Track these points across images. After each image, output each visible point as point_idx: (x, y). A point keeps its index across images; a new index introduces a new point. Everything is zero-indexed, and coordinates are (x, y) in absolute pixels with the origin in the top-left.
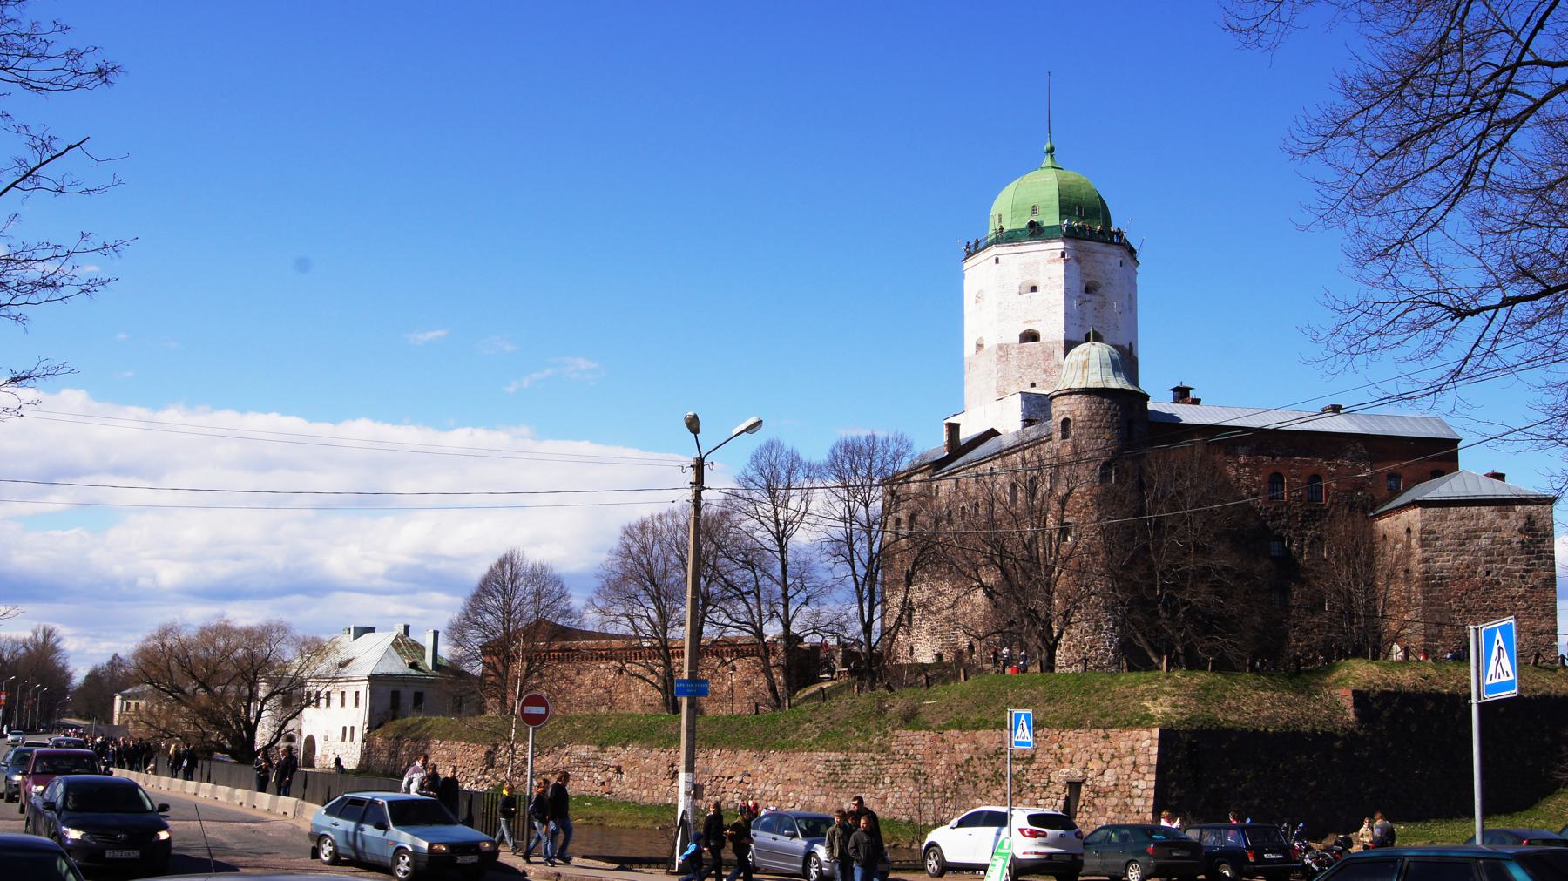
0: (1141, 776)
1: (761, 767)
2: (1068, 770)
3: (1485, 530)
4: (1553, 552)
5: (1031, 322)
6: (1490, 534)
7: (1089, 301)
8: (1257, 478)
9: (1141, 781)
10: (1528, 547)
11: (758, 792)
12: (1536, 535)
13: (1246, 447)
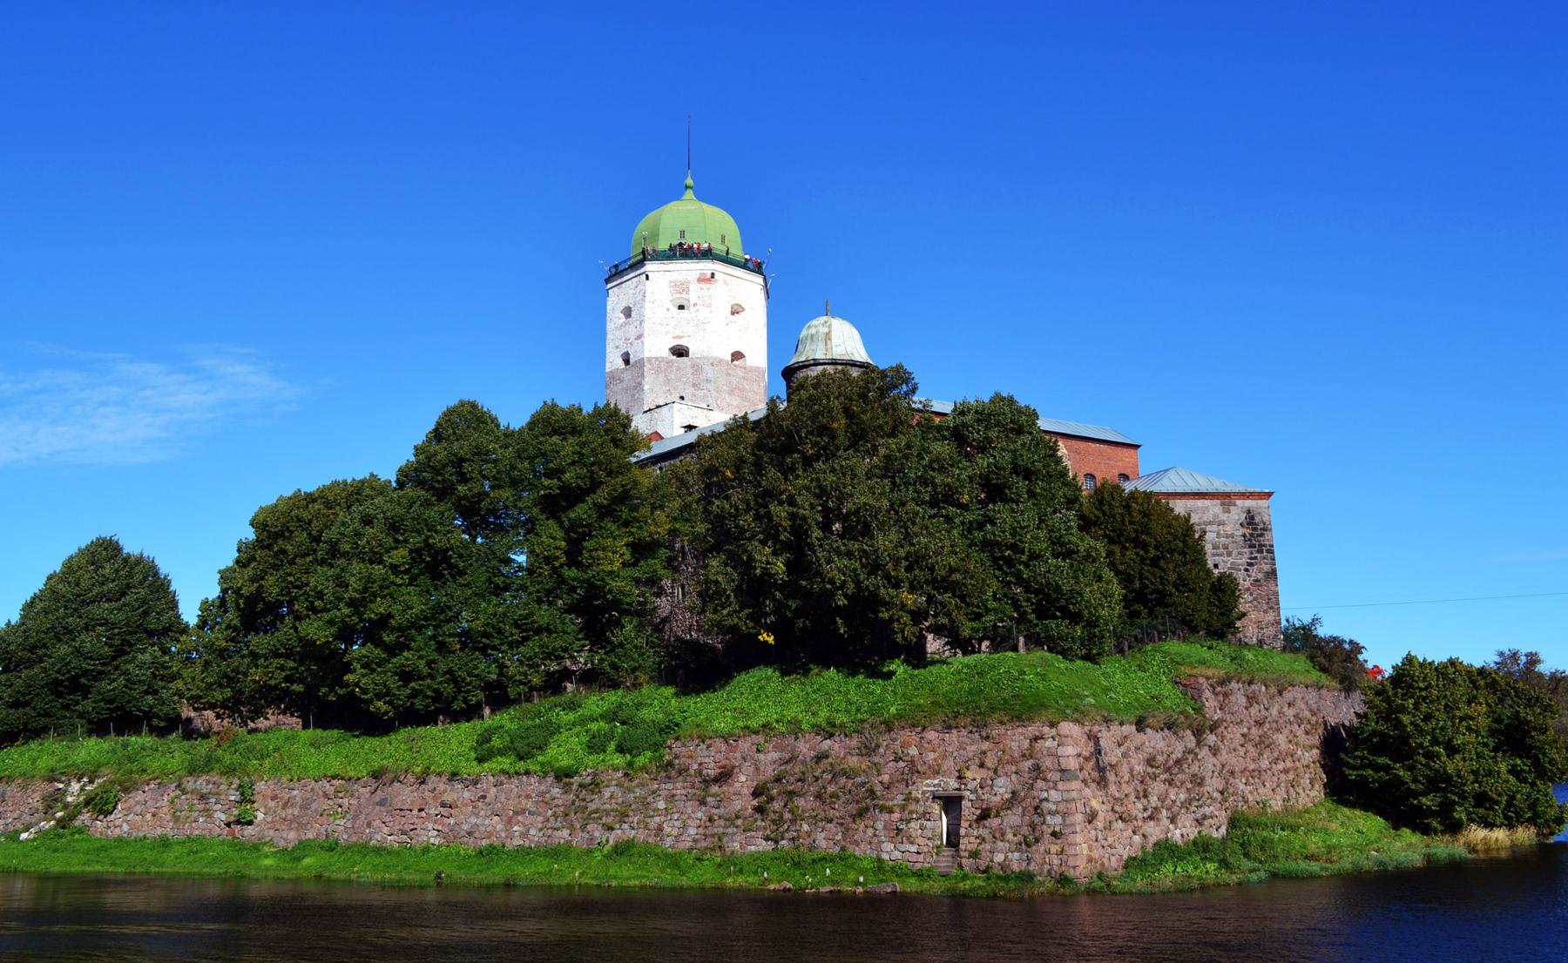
0: (1051, 784)
1: (467, 794)
2: (936, 782)
3: (1210, 523)
4: (1272, 546)
5: (680, 337)
6: (1214, 528)
9: (1052, 792)
10: (1250, 540)
11: (465, 827)
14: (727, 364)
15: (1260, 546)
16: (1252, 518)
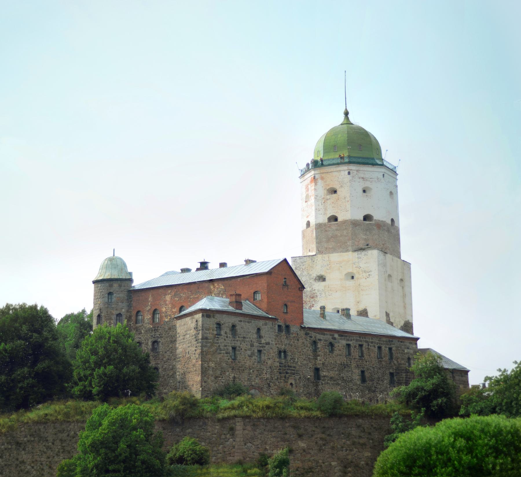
7: (330, 199)
8: (174, 310)
13: (170, 295)
14: (325, 225)
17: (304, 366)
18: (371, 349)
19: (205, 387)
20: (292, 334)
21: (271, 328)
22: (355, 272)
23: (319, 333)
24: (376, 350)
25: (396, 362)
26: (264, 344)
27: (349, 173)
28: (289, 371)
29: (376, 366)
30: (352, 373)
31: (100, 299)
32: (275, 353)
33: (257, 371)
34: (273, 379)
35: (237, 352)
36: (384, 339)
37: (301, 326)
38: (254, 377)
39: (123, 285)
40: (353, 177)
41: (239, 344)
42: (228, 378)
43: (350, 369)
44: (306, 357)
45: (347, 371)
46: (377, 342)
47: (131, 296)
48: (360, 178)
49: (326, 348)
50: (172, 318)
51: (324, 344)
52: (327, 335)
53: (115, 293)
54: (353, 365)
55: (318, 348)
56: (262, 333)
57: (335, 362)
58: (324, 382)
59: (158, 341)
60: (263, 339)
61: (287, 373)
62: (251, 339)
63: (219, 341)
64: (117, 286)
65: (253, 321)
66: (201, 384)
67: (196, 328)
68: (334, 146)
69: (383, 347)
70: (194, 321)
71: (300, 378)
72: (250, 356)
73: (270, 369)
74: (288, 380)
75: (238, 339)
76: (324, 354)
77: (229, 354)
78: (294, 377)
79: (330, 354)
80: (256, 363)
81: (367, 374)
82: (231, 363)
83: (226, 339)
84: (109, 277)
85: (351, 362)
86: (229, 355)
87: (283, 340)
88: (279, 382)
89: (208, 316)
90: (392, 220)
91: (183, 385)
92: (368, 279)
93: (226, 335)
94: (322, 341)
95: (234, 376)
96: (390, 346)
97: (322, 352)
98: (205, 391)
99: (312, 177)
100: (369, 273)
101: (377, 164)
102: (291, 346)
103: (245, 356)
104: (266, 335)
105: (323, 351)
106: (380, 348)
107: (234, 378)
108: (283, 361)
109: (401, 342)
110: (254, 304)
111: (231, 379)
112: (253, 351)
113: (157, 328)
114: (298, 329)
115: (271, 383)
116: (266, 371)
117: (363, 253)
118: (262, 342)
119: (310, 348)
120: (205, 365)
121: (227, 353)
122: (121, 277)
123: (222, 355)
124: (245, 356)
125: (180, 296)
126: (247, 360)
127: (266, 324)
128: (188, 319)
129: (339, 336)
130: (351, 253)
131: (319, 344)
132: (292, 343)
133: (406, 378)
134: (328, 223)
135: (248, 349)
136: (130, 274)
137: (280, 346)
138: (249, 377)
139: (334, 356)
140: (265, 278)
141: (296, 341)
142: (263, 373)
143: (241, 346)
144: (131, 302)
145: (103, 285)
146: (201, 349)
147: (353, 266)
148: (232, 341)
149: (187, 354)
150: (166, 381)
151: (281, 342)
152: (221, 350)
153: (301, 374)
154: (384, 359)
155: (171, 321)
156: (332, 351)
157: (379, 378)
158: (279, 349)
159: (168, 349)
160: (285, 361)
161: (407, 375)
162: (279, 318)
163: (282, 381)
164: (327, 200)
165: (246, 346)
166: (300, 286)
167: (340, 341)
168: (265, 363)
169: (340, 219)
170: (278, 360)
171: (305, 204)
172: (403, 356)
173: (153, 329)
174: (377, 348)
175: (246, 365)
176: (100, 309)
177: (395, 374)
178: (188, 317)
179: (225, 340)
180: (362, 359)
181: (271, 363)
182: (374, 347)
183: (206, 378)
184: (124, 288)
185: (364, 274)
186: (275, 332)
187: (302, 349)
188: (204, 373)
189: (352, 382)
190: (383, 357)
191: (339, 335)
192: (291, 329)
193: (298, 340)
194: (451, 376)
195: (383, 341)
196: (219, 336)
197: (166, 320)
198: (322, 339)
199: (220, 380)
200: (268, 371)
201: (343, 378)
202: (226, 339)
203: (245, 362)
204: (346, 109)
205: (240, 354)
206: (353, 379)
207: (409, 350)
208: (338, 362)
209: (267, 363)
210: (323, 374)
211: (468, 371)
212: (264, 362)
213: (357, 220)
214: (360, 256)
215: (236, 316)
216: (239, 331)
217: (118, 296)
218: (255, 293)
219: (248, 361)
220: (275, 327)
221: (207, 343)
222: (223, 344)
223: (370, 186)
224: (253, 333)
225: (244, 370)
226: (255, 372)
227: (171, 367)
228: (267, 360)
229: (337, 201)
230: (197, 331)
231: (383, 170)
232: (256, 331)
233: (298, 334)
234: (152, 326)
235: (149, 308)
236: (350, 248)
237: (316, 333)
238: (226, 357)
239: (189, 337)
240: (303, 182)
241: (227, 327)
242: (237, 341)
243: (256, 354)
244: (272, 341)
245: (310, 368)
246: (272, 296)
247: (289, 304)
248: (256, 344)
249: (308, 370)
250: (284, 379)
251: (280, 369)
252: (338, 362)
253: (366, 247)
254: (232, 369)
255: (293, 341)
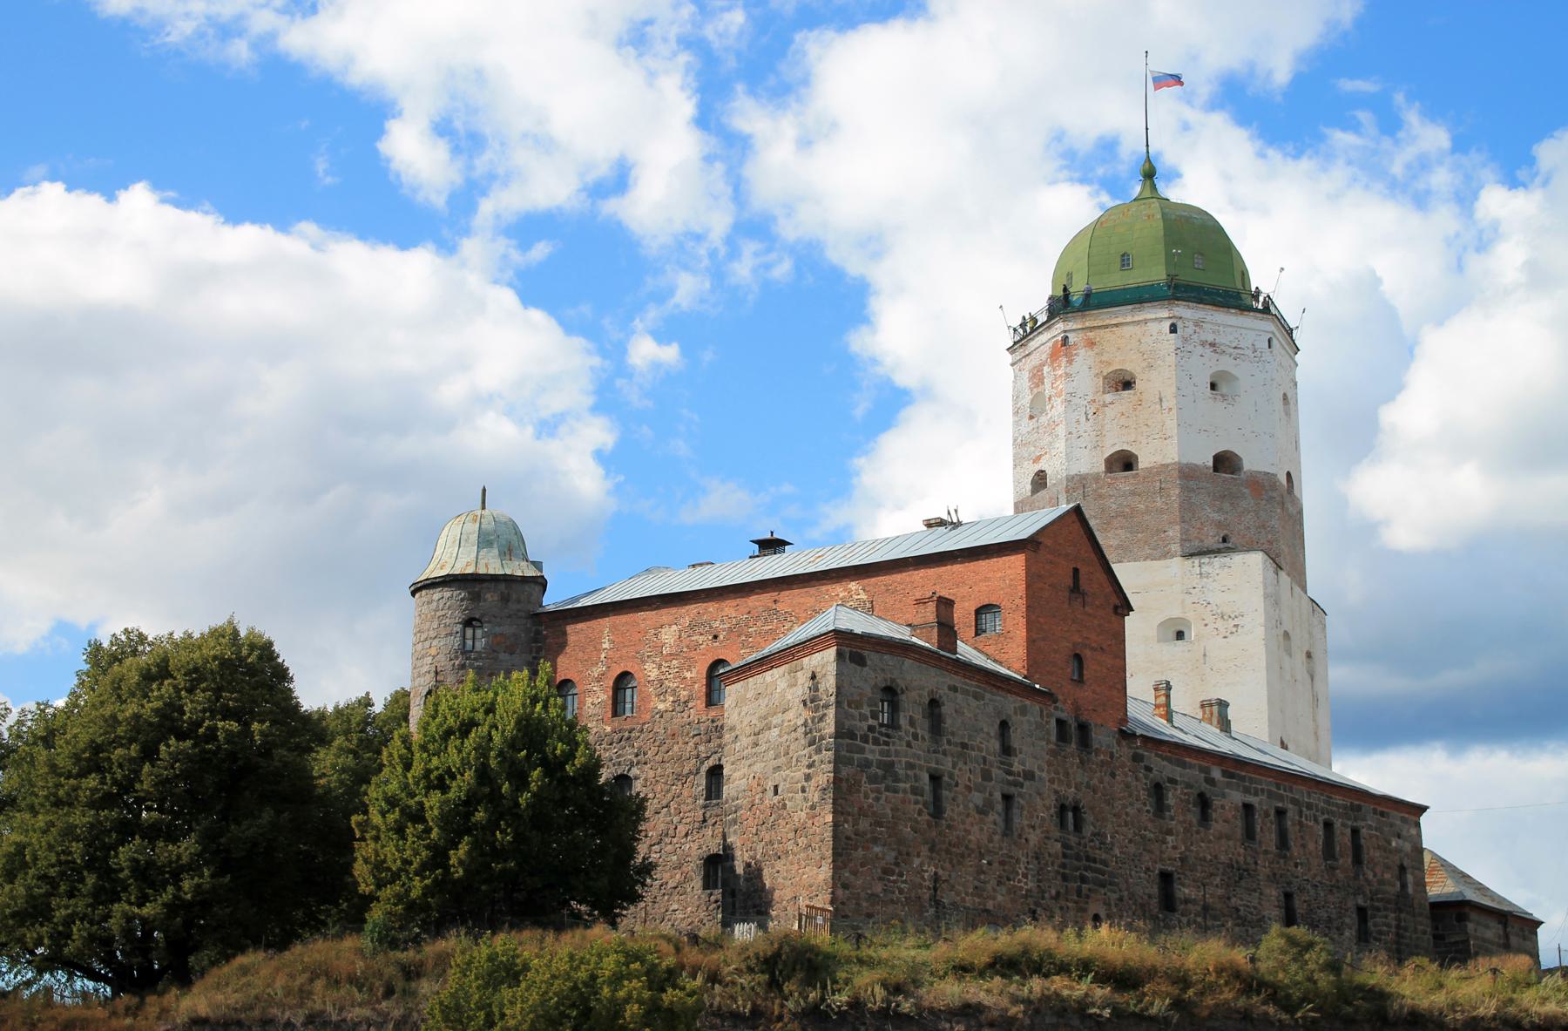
7: (1112, 403)
8: (688, 675)
12: (816, 709)
13: (674, 627)
14: (1096, 478)
15: (822, 738)
16: (817, 690)
17: (1132, 863)
18: (1307, 826)
19: (843, 903)
20: (1097, 752)
21: (1039, 726)
22: (1190, 616)
23: (1171, 762)
24: (1320, 830)
25: (1370, 875)
26: (1019, 773)
27: (1173, 329)
28: (1089, 874)
29: (1321, 883)
30: (1260, 899)
31: (436, 641)
32: (1048, 809)
33: (1002, 863)
34: (1047, 895)
35: (945, 793)
36: (1339, 800)
37: (1122, 732)
38: (993, 882)
39: (514, 596)
40: (1186, 340)
41: (950, 765)
42: (918, 880)
43: (1255, 886)
44: (1135, 834)
45: (1247, 889)
46: (1323, 808)
47: (538, 633)
48: (1203, 344)
49: (1189, 810)
50: (682, 700)
51: (1183, 797)
52: (1191, 766)
53: (489, 622)
54: (1264, 870)
55: (1169, 808)
56: (1015, 741)
57: (1216, 857)
58: (1185, 920)
59: (631, 775)
60: (1017, 760)
61: (1083, 880)
62: (984, 754)
63: (892, 748)
64: (496, 598)
65: (988, 696)
66: (833, 893)
67: (812, 701)
68: (1123, 255)
69: (1338, 823)
70: (803, 678)
71: (1121, 899)
72: (982, 811)
73: (1036, 862)
74: (1087, 903)
75: (947, 747)
76: (1185, 829)
77: (922, 796)
78: (1105, 894)
79: (1202, 829)
80: (997, 838)
81: (1300, 906)
82: (925, 826)
83: (914, 743)
84: (470, 570)
85: (1256, 863)
86: (920, 798)
87: (1070, 771)
88: (1061, 908)
89: (859, 660)
90: (1289, 474)
91: (750, 903)
92: (1231, 639)
93: (912, 730)
94: (1179, 787)
95: (936, 873)
96: (1355, 824)
97: (1180, 822)
98: (843, 917)
99: (1057, 341)
100: (1236, 622)
101: (1251, 309)
102: (1095, 791)
103: (966, 807)
104: (1024, 749)
105: (1181, 819)
106: (1328, 825)
107: (936, 878)
108: (1073, 840)
109: (1382, 814)
110: (975, 648)
111: (927, 883)
112: (991, 795)
113: (627, 734)
114: (1114, 737)
115: (1039, 911)
116: (1026, 868)
117: (1218, 561)
118: (1014, 769)
119: (1145, 804)
120: (846, 826)
121: (915, 791)
122: (509, 572)
123: (901, 795)
124: (966, 807)
125: (711, 627)
126: (972, 825)
127: (1023, 711)
128: (775, 677)
129: (1223, 776)
130: (1178, 560)
131: (1170, 795)
132: (1095, 781)
133: (1398, 927)
134: (1106, 472)
135: (975, 784)
136: (538, 565)
137: (1062, 789)
138: (976, 883)
139: (1211, 837)
140: (1017, 562)
141: (1107, 779)
142: (1018, 874)
143: (956, 772)
144: (537, 652)
145: (447, 594)
146: (835, 772)
147: (1183, 601)
148: (929, 751)
149: (770, 793)
150: (656, 905)
151: (1067, 774)
152: (897, 780)
153: (1123, 886)
154: (1341, 861)
155: (678, 709)
156: (1205, 818)
157: (1330, 920)
158: (1059, 796)
159: (664, 802)
160: (1077, 840)
161: (1398, 919)
162: (1060, 697)
163: (1070, 905)
164: (1105, 405)
165: (968, 774)
166: (1117, 602)
167: (1227, 790)
168: (1024, 841)
169: (1144, 462)
170: (1059, 834)
171: (1027, 425)
172: (1387, 858)
173: (616, 737)
174: (1322, 825)
175: (970, 841)
176: (437, 673)
177: (1369, 912)
178: (772, 667)
179: (909, 745)
180: (1285, 857)
181: (1039, 842)
182: (1316, 820)
183: (847, 875)
184: (519, 607)
185: (1220, 624)
186: (1049, 742)
187: (1124, 806)
188: (841, 855)
189: (1261, 926)
190: (1337, 856)
191: (1225, 773)
192: (1094, 735)
193: (1113, 775)
194: (1501, 933)
195: (1337, 805)
196: (890, 731)
197: (661, 706)
198: (1178, 779)
199: (895, 882)
200: (1031, 866)
201: (1238, 910)
202: (914, 743)
203: (965, 830)
204: (1148, 159)
205: (954, 800)
206: (1264, 917)
207: (1400, 841)
208: (1223, 858)
209: (1026, 840)
210: (1184, 893)
211: (1540, 923)
212: (1020, 836)
213: (1196, 465)
214: (1205, 569)
215: (941, 668)
216: (949, 721)
217: (498, 630)
218: (978, 612)
219: (976, 828)
220: (1047, 722)
221: (851, 752)
222: (904, 760)
223: (1234, 371)
224: (988, 734)
225: (963, 856)
226: (996, 865)
227: (675, 858)
228: (1026, 828)
229: (1135, 410)
230: (816, 709)
231: (1268, 326)
232: (994, 730)
233: (1112, 755)
234: (608, 729)
235: (596, 671)
236: (1175, 547)
237: (1160, 756)
238: (912, 806)
239: (780, 736)
240: (1020, 360)
241: (916, 702)
242: (945, 753)
243: (999, 807)
244: (1039, 768)
245: (1148, 869)
246: (1041, 620)
247: (1087, 654)
248: (996, 772)
249: (1142, 875)
250: (1076, 898)
251: (1063, 866)
252: (1223, 858)
253: (1222, 546)
254: (932, 850)
255: (1098, 774)
